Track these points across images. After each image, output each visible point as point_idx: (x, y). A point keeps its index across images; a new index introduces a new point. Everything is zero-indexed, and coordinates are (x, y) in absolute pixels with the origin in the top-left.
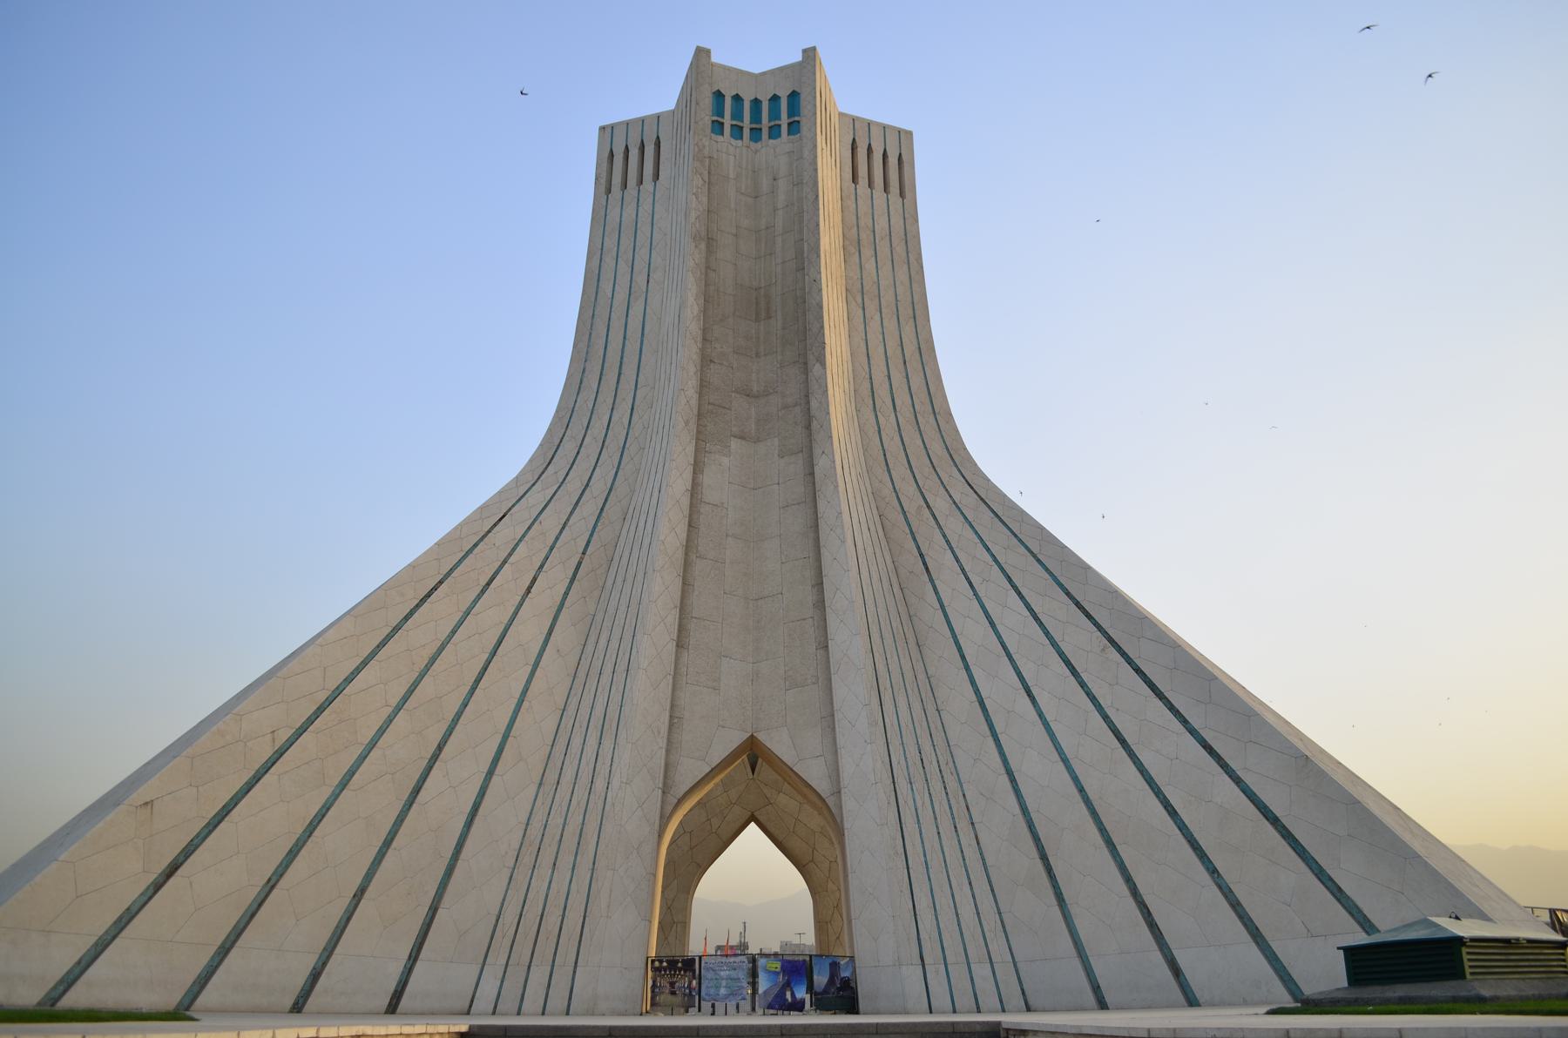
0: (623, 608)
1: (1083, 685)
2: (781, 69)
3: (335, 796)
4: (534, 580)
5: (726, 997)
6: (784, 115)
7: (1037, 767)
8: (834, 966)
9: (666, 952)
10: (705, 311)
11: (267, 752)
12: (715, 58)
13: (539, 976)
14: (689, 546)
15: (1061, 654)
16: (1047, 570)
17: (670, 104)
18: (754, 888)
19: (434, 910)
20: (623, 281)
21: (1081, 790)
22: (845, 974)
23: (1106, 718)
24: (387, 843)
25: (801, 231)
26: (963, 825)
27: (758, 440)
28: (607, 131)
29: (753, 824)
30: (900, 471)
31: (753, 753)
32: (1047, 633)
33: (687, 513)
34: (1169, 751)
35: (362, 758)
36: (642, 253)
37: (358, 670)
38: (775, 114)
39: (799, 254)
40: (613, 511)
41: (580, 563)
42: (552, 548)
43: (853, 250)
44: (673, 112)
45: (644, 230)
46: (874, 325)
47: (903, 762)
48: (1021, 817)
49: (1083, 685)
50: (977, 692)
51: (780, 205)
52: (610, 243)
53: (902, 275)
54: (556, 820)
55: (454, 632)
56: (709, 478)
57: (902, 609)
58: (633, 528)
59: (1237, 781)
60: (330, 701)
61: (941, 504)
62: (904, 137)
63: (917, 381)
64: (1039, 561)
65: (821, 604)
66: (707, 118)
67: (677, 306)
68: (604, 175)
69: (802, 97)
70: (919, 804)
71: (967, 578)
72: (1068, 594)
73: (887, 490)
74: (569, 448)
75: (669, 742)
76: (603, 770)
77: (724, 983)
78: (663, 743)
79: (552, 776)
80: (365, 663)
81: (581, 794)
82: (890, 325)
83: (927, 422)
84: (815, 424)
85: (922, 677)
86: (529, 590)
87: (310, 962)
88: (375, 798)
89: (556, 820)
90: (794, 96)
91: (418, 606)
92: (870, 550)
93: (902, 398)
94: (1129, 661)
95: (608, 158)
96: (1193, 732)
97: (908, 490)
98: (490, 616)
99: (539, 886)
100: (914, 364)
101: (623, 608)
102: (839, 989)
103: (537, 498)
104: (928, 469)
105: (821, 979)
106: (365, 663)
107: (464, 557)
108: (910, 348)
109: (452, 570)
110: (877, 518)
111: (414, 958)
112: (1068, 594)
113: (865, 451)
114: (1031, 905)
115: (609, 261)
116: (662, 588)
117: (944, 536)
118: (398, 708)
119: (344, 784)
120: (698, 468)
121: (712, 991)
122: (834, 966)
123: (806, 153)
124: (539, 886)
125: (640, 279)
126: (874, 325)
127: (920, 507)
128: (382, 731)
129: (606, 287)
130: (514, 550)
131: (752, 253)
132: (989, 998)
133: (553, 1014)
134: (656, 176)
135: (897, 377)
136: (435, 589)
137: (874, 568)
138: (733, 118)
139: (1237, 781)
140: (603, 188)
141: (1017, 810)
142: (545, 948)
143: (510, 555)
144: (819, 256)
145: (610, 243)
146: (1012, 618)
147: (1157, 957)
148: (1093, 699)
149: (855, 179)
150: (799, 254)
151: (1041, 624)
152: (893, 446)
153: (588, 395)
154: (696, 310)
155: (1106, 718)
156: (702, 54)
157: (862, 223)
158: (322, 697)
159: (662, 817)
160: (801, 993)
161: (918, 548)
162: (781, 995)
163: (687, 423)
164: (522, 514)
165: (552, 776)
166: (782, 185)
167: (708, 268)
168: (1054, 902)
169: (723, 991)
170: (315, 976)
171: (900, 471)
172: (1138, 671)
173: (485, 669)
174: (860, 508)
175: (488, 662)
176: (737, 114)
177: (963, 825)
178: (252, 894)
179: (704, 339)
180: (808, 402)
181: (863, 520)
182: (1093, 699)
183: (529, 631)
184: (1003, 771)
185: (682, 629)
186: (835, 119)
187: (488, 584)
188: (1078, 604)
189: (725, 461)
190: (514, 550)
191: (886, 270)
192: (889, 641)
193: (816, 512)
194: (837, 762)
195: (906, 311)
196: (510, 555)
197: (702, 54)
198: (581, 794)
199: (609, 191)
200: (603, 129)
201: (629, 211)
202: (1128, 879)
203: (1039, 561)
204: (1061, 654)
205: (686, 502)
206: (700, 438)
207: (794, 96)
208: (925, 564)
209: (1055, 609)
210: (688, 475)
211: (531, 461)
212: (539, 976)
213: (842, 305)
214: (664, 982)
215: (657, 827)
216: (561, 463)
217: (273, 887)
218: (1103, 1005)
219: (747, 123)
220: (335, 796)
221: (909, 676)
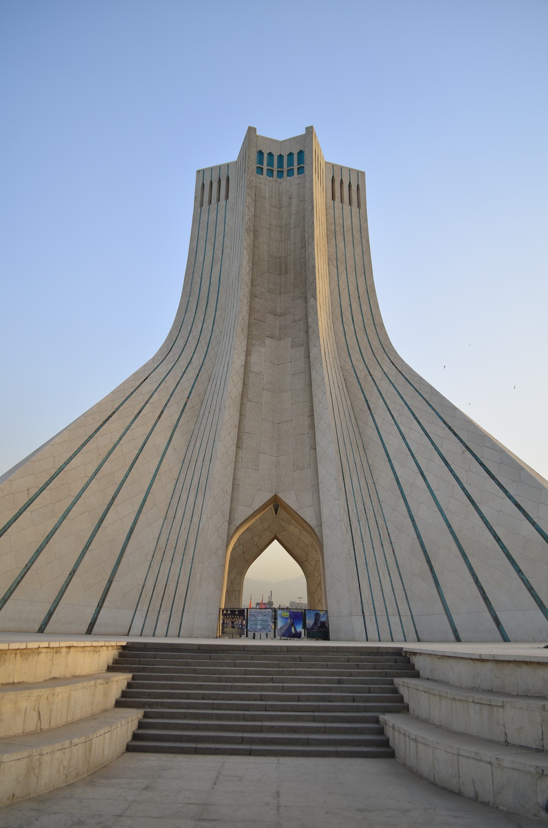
0: (208, 427)
1: (451, 471)
2: (294, 138)
3: (60, 523)
4: (162, 412)
5: (260, 630)
6: (296, 163)
7: (426, 514)
8: (317, 616)
9: (230, 606)
10: (252, 270)
11: (25, 500)
12: (258, 133)
13: (164, 617)
14: (243, 395)
15: (440, 455)
16: (434, 409)
17: (235, 159)
18: (276, 573)
19: (110, 582)
20: (209, 254)
21: (449, 527)
22: (323, 619)
23: (464, 489)
24: (87, 547)
25: (304, 227)
26: (386, 543)
27: (280, 339)
28: (201, 173)
29: (276, 541)
30: (356, 355)
31: (276, 503)
32: (433, 443)
33: (242, 377)
34: (496, 506)
35: (74, 503)
36: (219, 239)
37: (71, 458)
38: (290, 163)
39: (303, 239)
40: (203, 376)
41: (186, 404)
42: (171, 396)
43: (332, 236)
44: (236, 162)
45: (220, 226)
46: (343, 277)
47: (355, 510)
48: (417, 541)
49: (451, 471)
50: (395, 473)
51: (293, 213)
52: (202, 233)
53: (358, 250)
54: (173, 537)
55: (120, 439)
56: (253, 359)
57: (356, 429)
58: (214, 385)
59: (534, 524)
60: (57, 474)
61: (377, 374)
62: (360, 175)
63: (365, 308)
64: (429, 404)
65: (312, 426)
66: (254, 165)
67: (237, 266)
68: (199, 197)
69: (305, 153)
70: (363, 531)
71: (391, 414)
72: (445, 422)
73: (349, 366)
74: (180, 342)
75: (232, 497)
76: (198, 511)
77: (259, 623)
78: (229, 498)
79: (171, 514)
80: (75, 455)
81: (186, 523)
82: (352, 277)
83: (370, 329)
84: (310, 330)
85: (365, 465)
86: (159, 417)
87: (47, 607)
88: (80, 525)
89: (173, 537)
90: (301, 153)
91: (102, 425)
92: (339, 398)
93: (358, 317)
94: (477, 459)
95: (201, 188)
96: (510, 497)
97: (360, 366)
98: (139, 431)
99: (165, 570)
100: (364, 299)
101: (208, 427)
102: (319, 627)
103: (164, 369)
104: (371, 355)
105: (310, 622)
106: (75, 455)
107: (126, 400)
108: (362, 290)
109: (119, 407)
110: (343, 380)
111: (100, 606)
112: (445, 422)
113: (337, 344)
114: (422, 586)
115: (202, 243)
116: (228, 418)
117: (379, 391)
118: (92, 478)
119: (64, 517)
120: (248, 354)
121: (253, 627)
122: (317, 616)
123: (307, 184)
124: (165, 570)
125: (218, 253)
126: (343, 277)
127: (366, 375)
128: (83, 490)
129: (200, 257)
130: (152, 396)
131: (277, 238)
132: (398, 634)
133: (171, 636)
134: (227, 197)
135: (355, 306)
136: (111, 416)
137: (341, 407)
138: (268, 165)
139: (534, 524)
140: (199, 204)
141: (415, 537)
142: (167, 602)
143: (150, 399)
144: (313, 240)
145: (202, 233)
146: (415, 435)
147: (488, 615)
148: (457, 479)
149: (333, 198)
150: (303, 239)
151: (429, 438)
152: (352, 342)
153: (190, 315)
154: (248, 268)
155: (464, 489)
156: (251, 130)
157: (337, 222)
158: (53, 472)
159: (228, 536)
160: (300, 629)
161: (365, 397)
162: (289, 629)
163: (242, 329)
164: (156, 377)
165: (171, 514)
166: (294, 201)
167: (254, 246)
168: (434, 585)
169: (259, 627)
170: (50, 614)
171: (356, 355)
172: (481, 464)
173: (137, 458)
174: (334, 375)
175: (138, 455)
176: (270, 163)
177: (386, 543)
178: (18, 572)
179: (252, 285)
180: (307, 319)
181: (335, 381)
182: (457, 479)
183: (159, 439)
184: (408, 516)
185: (239, 438)
186: (323, 165)
187: (138, 414)
188: (450, 428)
189: (263, 349)
190: (152, 396)
191: (349, 248)
192: (348, 446)
193: (310, 377)
194: (320, 509)
195: (360, 270)
196: (150, 399)
197: (251, 130)
198: (186, 523)
199: (202, 205)
200: (198, 172)
201: (213, 216)
202: (473, 574)
203: (429, 404)
204: (440, 455)
205: (242, 371)
206: (250, 338)
207: (301, 153)
208: (368, 405)
209: (438, 430)
210: (243, 357)
211: (160, 349)
212: (164, 617)
213: (326, 266)
214: (229, 622)
215: (225, 541)
216: (176, 350)
217: (28, 569)
218: (458, 640)
220: (60, 523)
221: (359, 464)
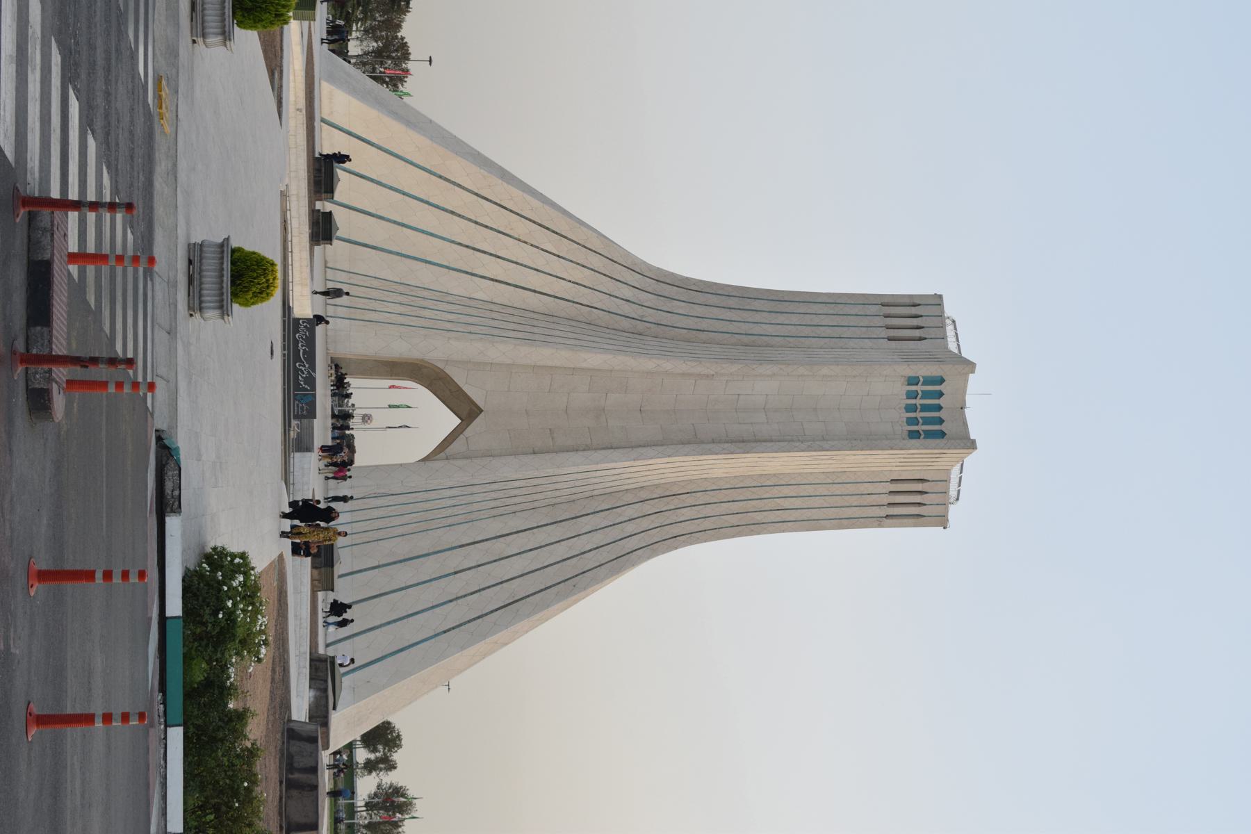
28: (937, 300)
38: (927, 421)
90: (942, 434)
95: (913, 305)
140: (886, 300)
176: (926, 395)
200: (940, 297)
207: (942, 434)
219: (919, 402)
